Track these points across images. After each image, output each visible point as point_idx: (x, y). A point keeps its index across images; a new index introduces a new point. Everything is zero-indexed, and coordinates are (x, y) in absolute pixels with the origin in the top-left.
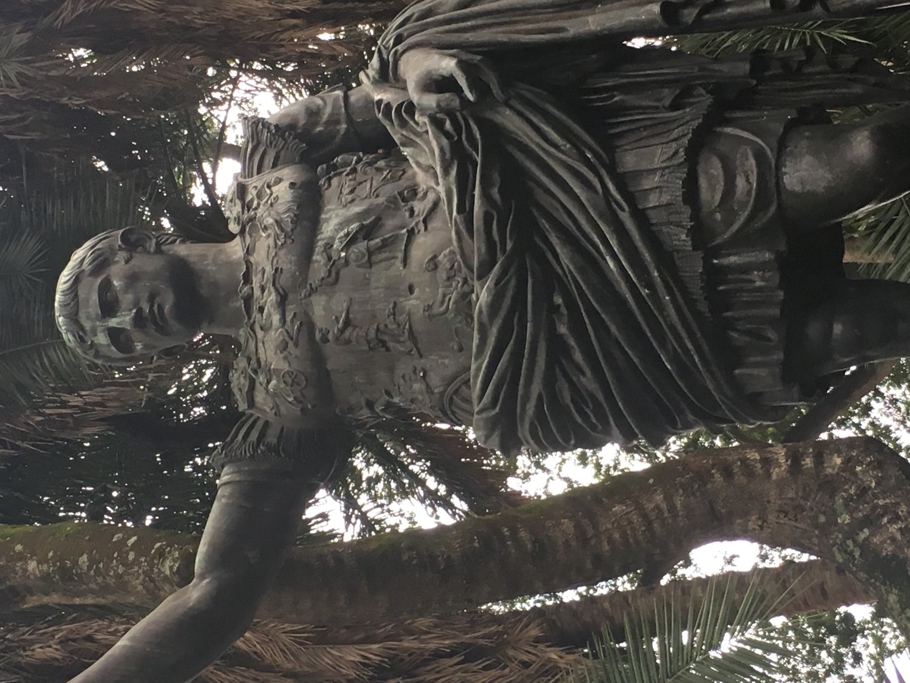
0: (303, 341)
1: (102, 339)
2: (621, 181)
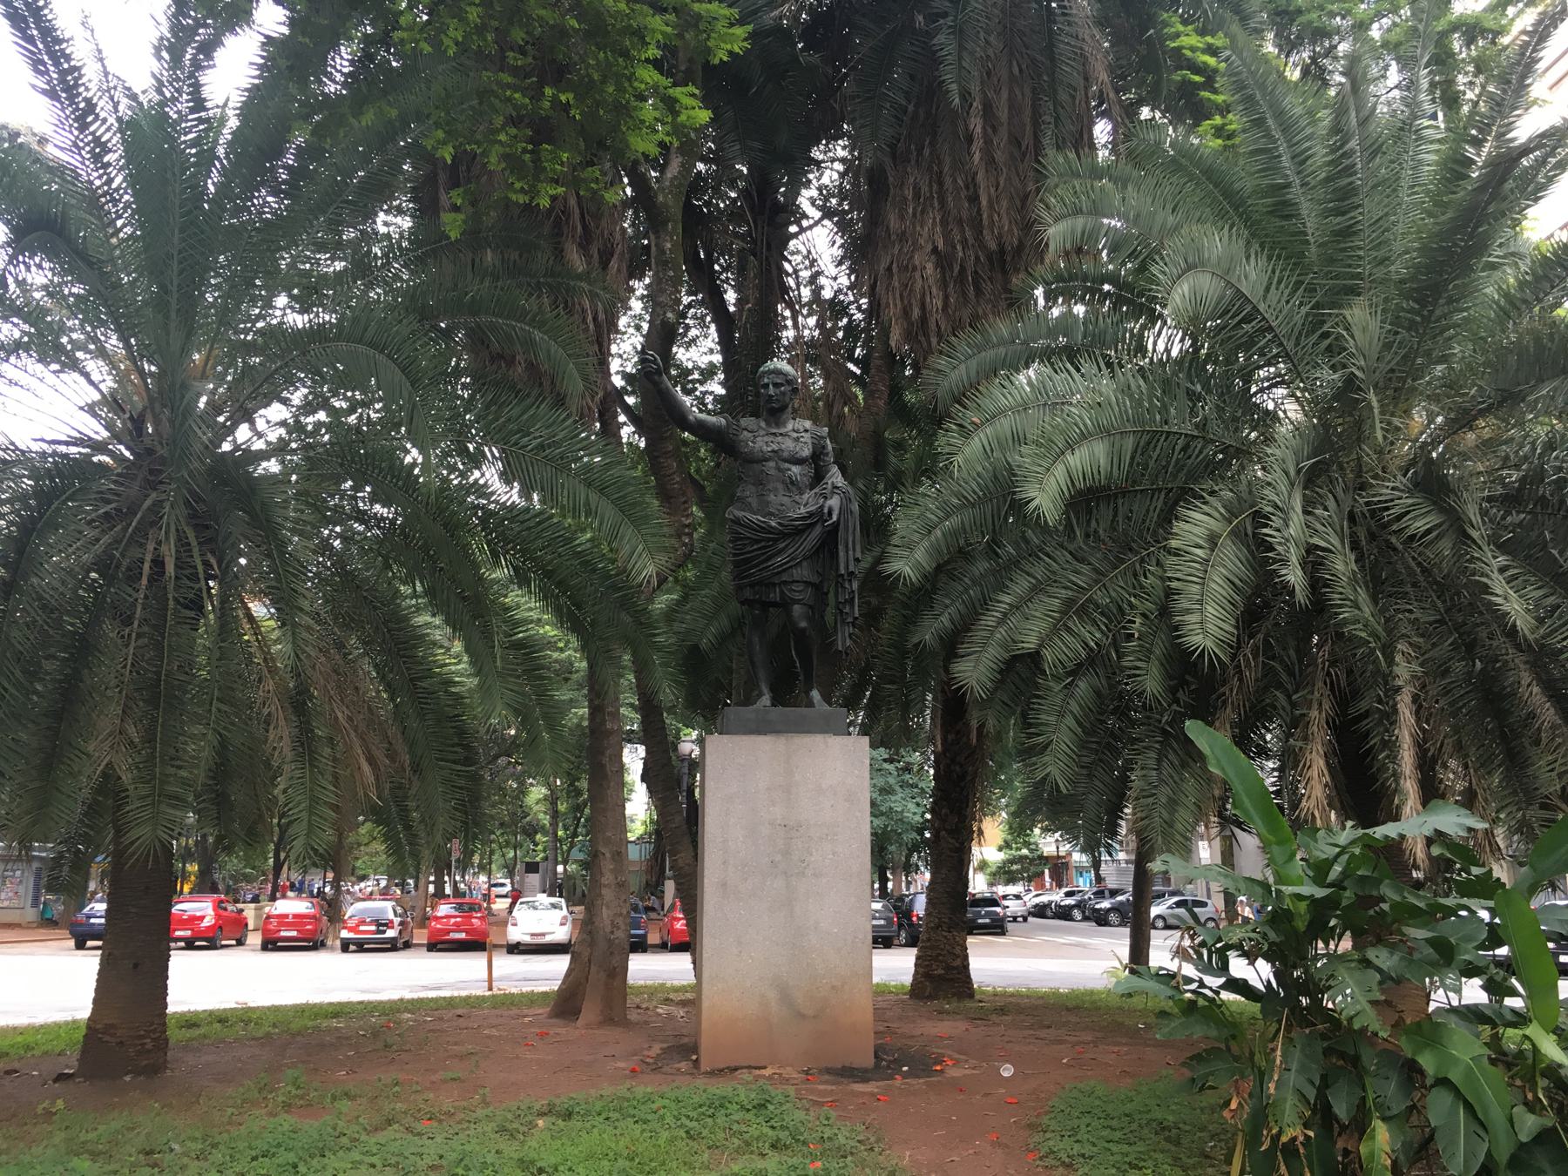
1: (766, 380)
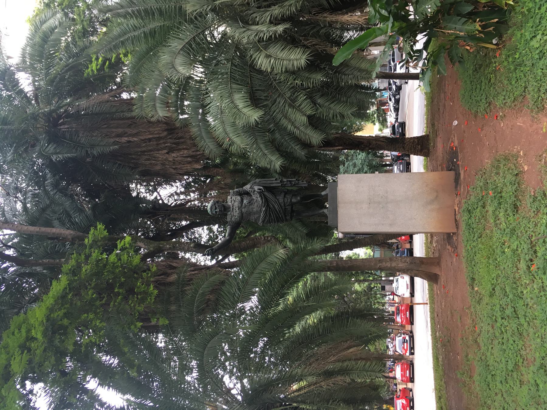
1: (214, 212)
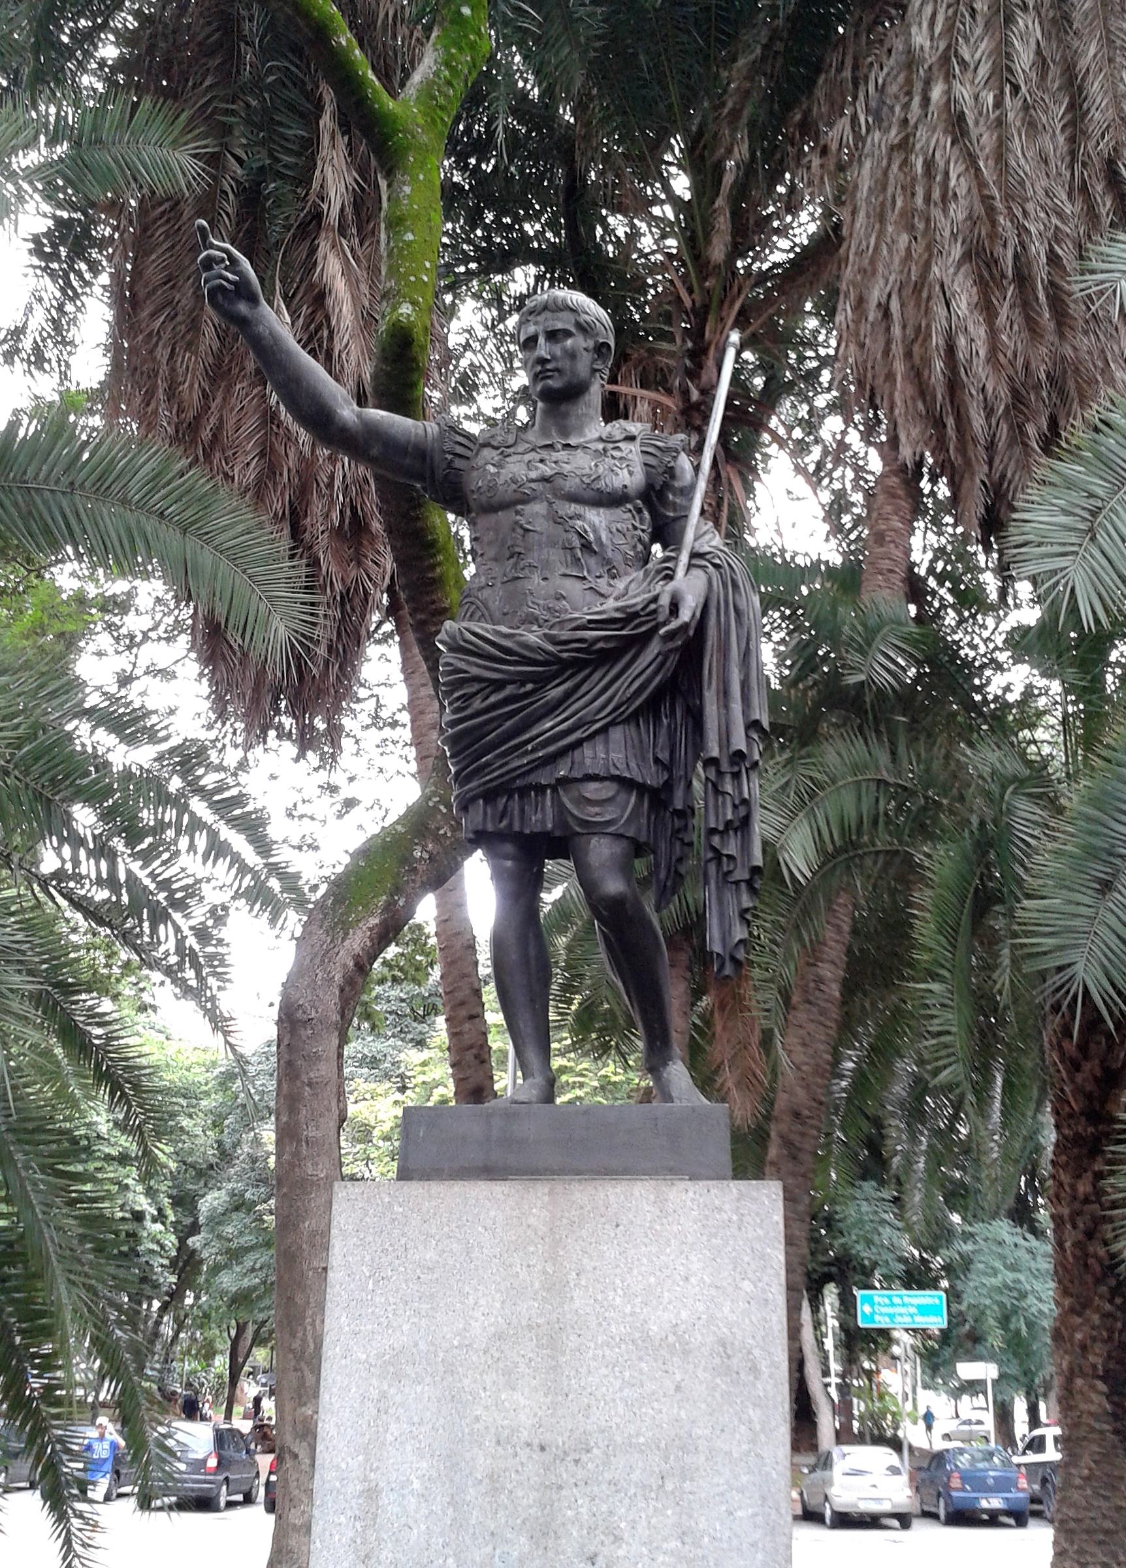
0: (518, 496)
1: (531, 329)
2: (604, 730)
